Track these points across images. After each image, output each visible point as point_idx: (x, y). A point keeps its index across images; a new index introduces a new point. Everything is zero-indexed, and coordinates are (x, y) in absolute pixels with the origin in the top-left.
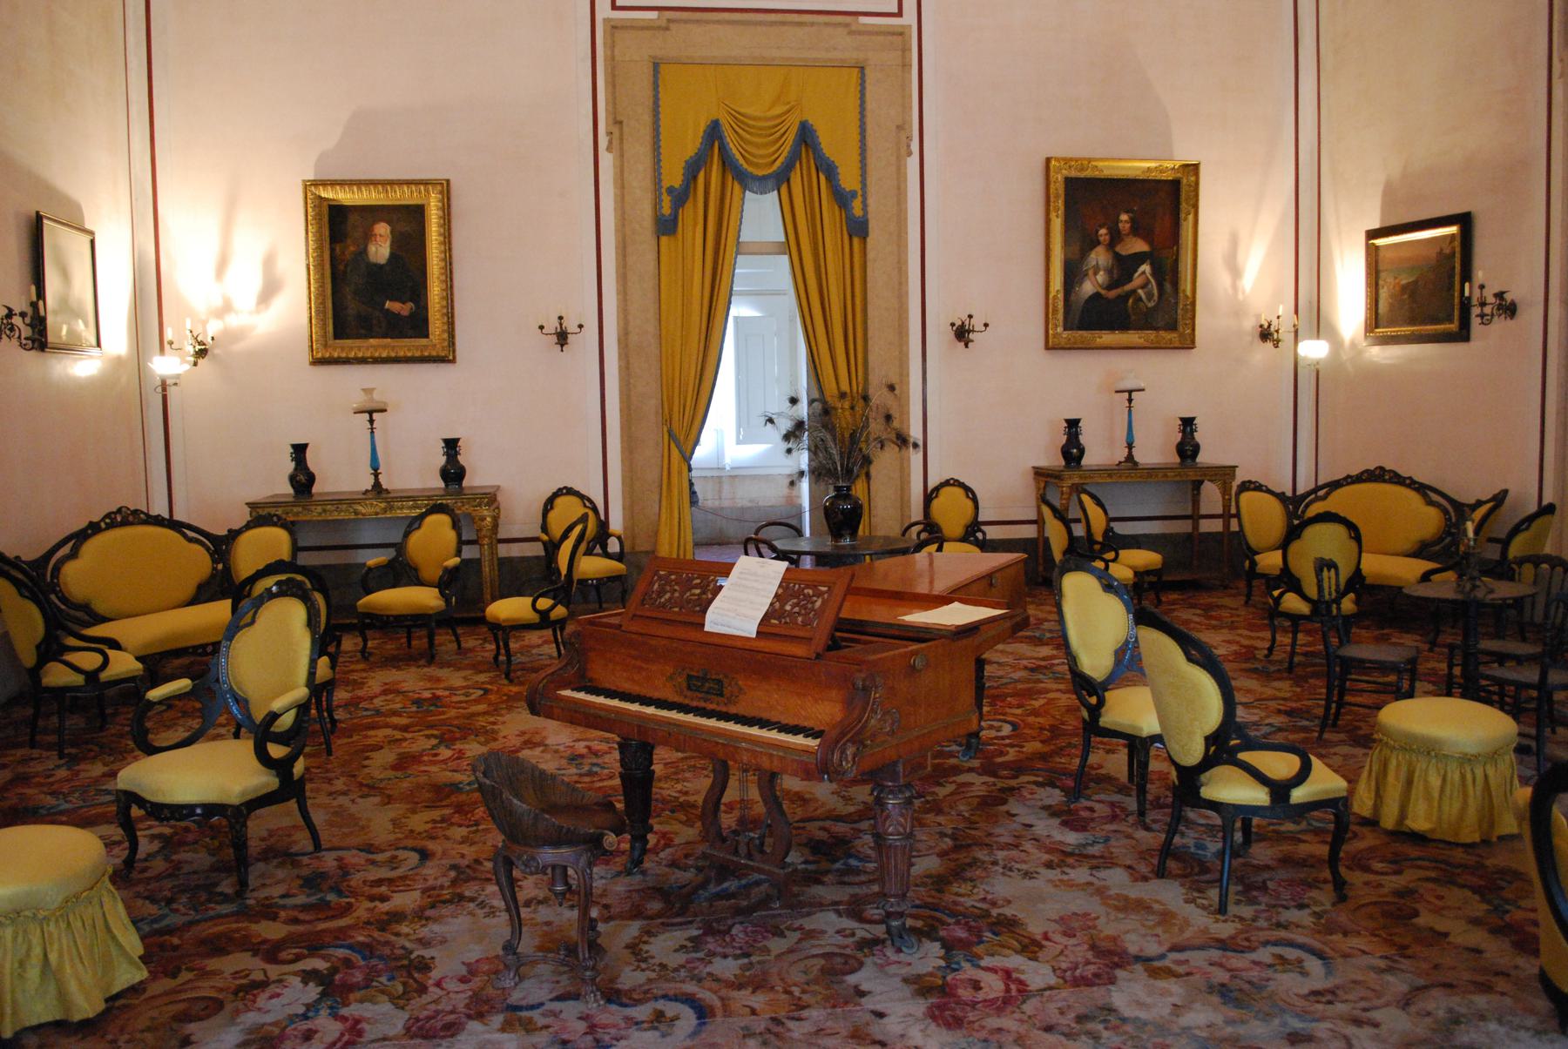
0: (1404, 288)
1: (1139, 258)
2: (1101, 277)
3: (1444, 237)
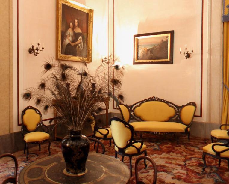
0: (148, 50)
1: (79, 34)
2: (71, 38)
3: (163, 37)
